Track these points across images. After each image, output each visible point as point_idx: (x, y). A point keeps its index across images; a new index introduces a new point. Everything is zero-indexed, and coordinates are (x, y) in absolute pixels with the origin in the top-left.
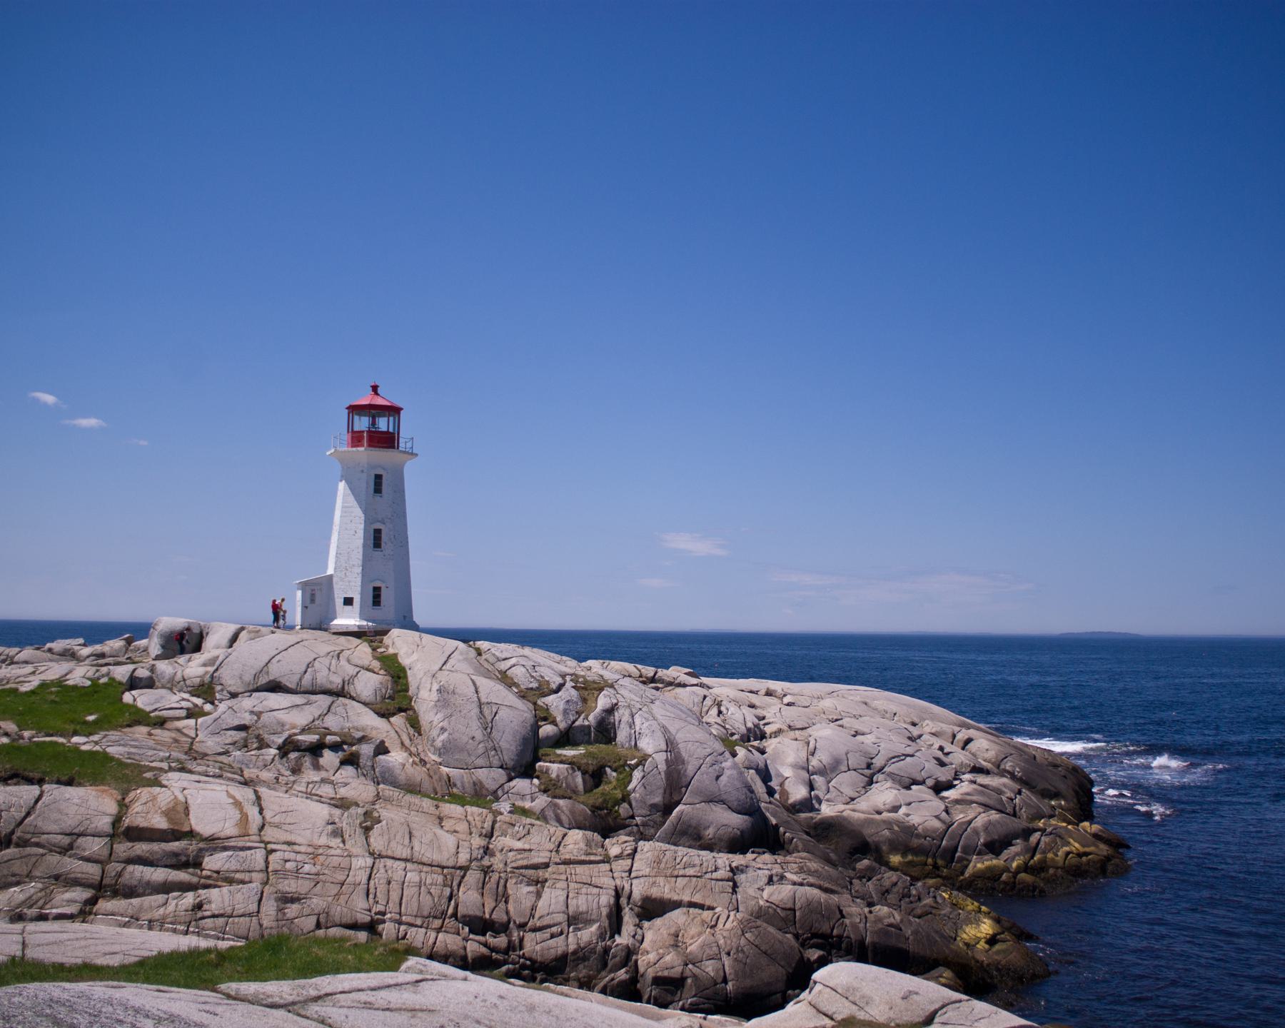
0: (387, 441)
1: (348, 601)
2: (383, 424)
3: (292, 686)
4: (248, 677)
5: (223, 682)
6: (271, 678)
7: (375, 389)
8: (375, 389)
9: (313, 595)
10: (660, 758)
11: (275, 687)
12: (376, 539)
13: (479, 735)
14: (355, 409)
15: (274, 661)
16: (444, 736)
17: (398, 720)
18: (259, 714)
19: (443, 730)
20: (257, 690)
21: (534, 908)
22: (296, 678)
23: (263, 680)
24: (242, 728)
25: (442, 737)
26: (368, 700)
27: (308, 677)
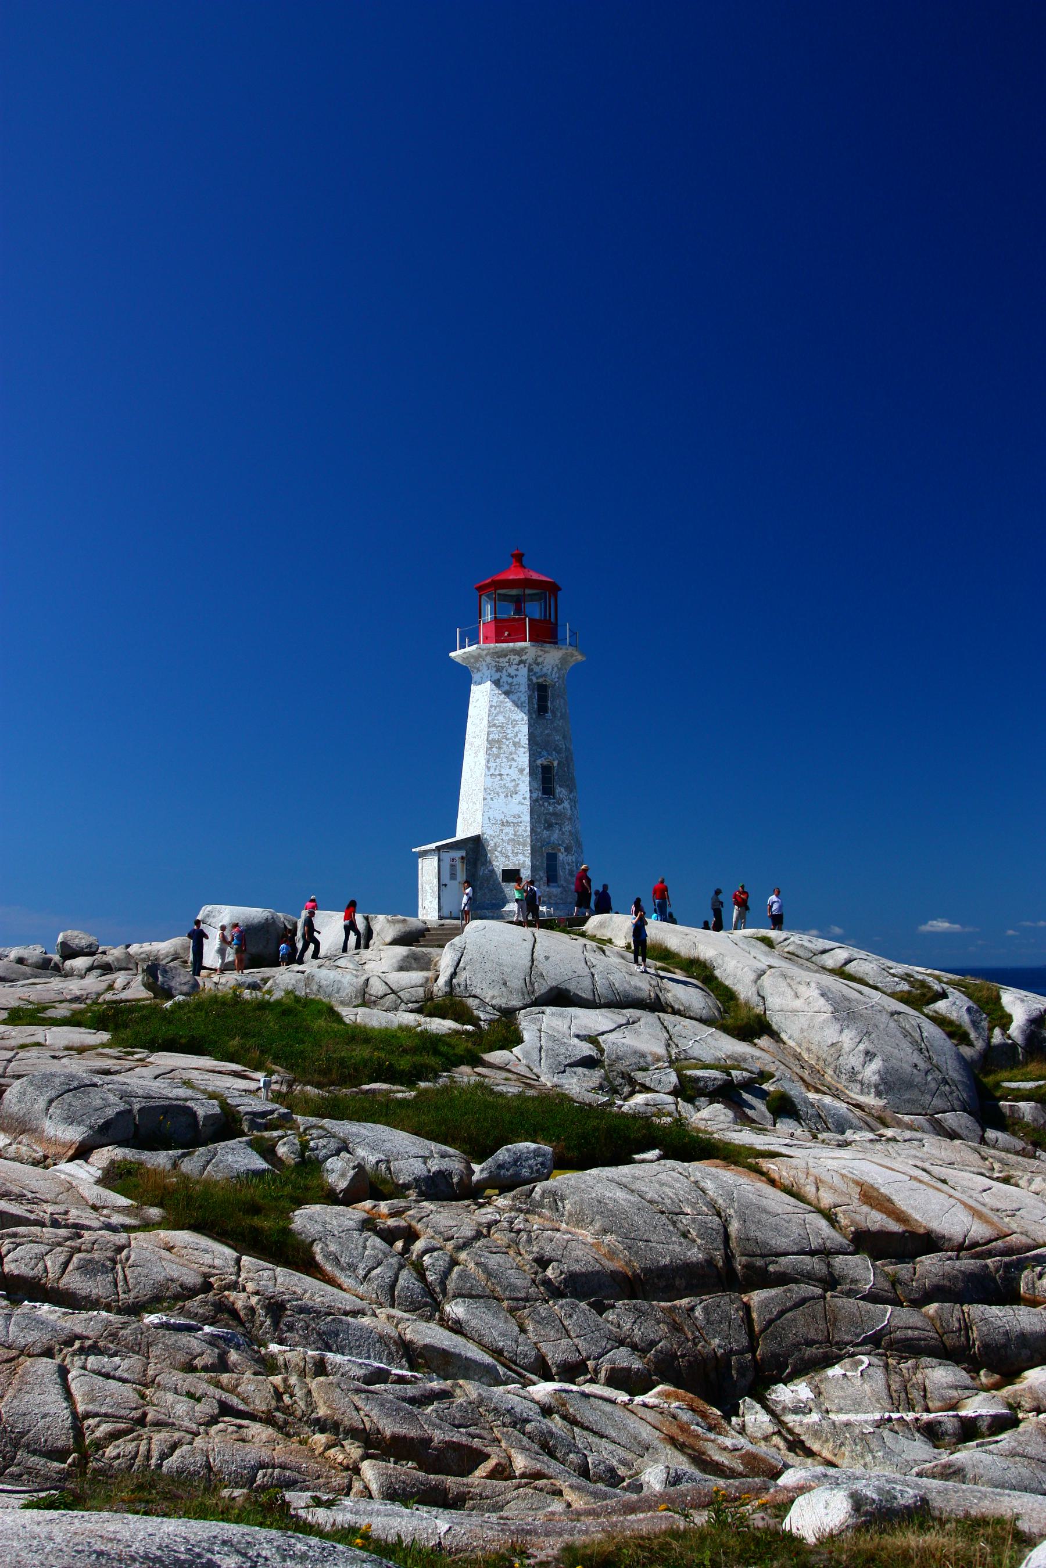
3: (587, 995)
4: (516, 983)
5: (477, 991)
6: (554, 984)
8: (519, 558)
11: (560, 997)
13: (922, 1065)
16: (876, 1065)
17: (764, 1041)
18: (592, 1040)
19: (869, 1055)
20: (534, 1004)
22: (587, 983)
23: (541, 988)
24: (589, 1063)
25: (876, 1065)
26: (705, 1013)
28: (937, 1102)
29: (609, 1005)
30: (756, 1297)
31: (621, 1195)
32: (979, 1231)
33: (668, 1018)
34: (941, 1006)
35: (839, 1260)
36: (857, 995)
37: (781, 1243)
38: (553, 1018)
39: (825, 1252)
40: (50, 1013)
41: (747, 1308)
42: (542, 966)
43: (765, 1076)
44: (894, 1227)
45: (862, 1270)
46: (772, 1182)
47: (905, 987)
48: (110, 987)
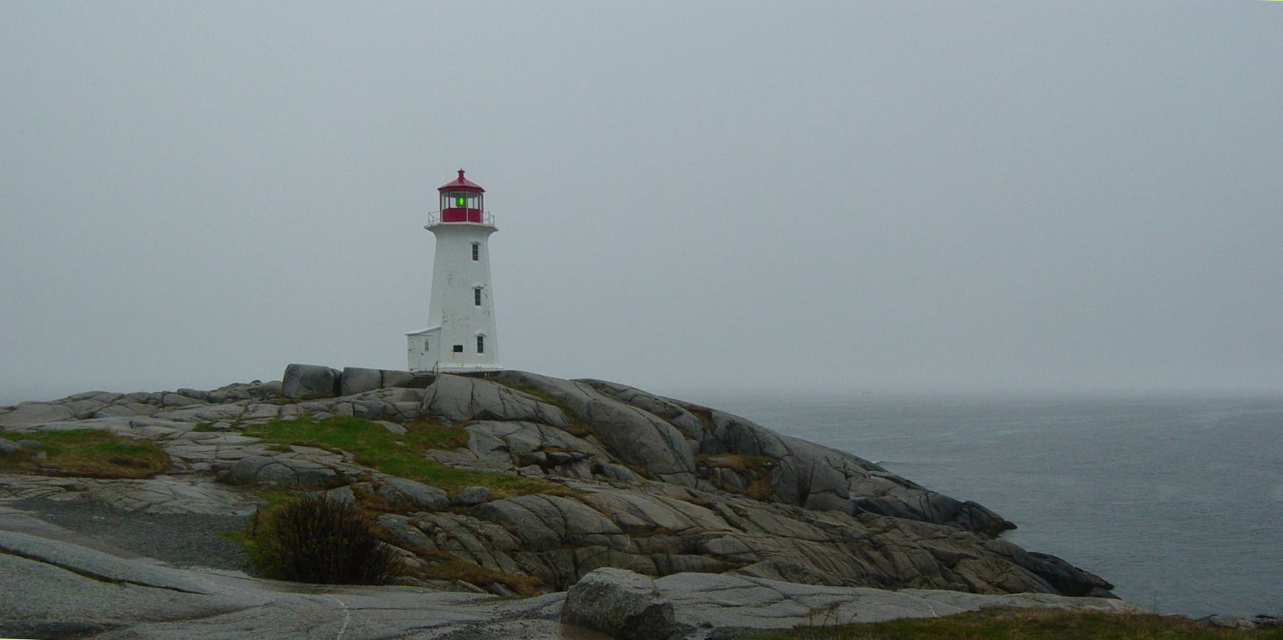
1: (458, 349)
2: (472, 203)
4: (464, 409)
7: (461, 173)
8: (461, 173)
9: (427, 344)
10: (788, 459)
11: (488, 416)
14: (446, 191)
15: (476, 394)
17: (590, 437)
18: (503, 437)
21: (894, 566)
22: (500, 408)
23: (477, 412)
27: (508, 407)
28: (676, 468)
29: (511, 420)
30: (578, 551)
31: (520, 509)
32: (681, 525)
33: (543, 427)
35: (614, 537)
36: (636, 414)
37: (590, 529)
38: (485, 427)
39: (609, 533)
40: (217, 425)
41: (575, 556)
42: (480, 400)
43: (587, 456)
44: (642, 523)
45: (627, 541)
46: (588, 504)
47: (661, 410)
48: (246, 410)
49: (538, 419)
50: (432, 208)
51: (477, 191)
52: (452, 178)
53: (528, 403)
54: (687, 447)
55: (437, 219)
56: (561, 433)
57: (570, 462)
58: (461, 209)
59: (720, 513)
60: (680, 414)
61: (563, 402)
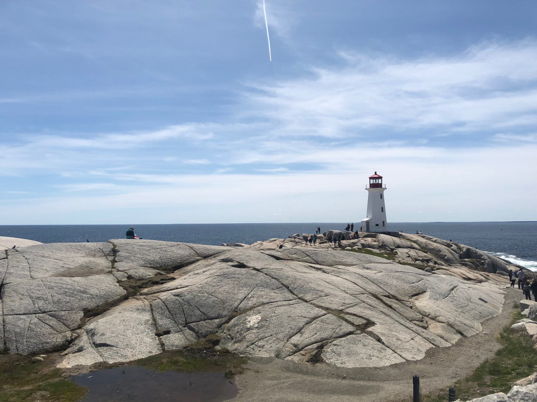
0: (380, 185)
1: (377, 225)
8: (376, 173)
10: (489, 260)
12: (383, 209)
34: (452, 248)
49: (412, 247)
50: (367, 183)
51: (381, 178)
52: (372, 174)
53: (409, 243)
54: (457, 255)
55: (368, 187)
56: (421, 252)
57: (428, 261)
58: (376, 184)
59: (482, 275)
60: (452, 246)
61: (415, 242)
